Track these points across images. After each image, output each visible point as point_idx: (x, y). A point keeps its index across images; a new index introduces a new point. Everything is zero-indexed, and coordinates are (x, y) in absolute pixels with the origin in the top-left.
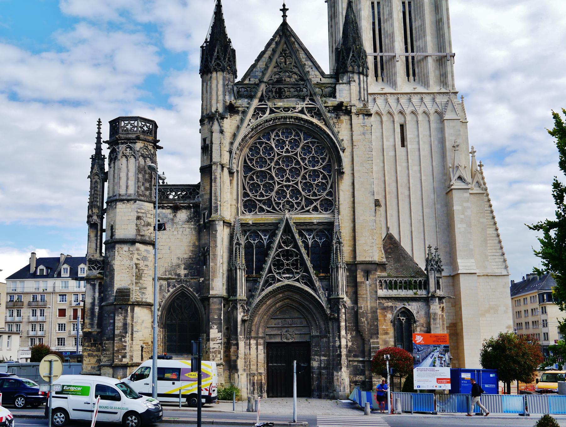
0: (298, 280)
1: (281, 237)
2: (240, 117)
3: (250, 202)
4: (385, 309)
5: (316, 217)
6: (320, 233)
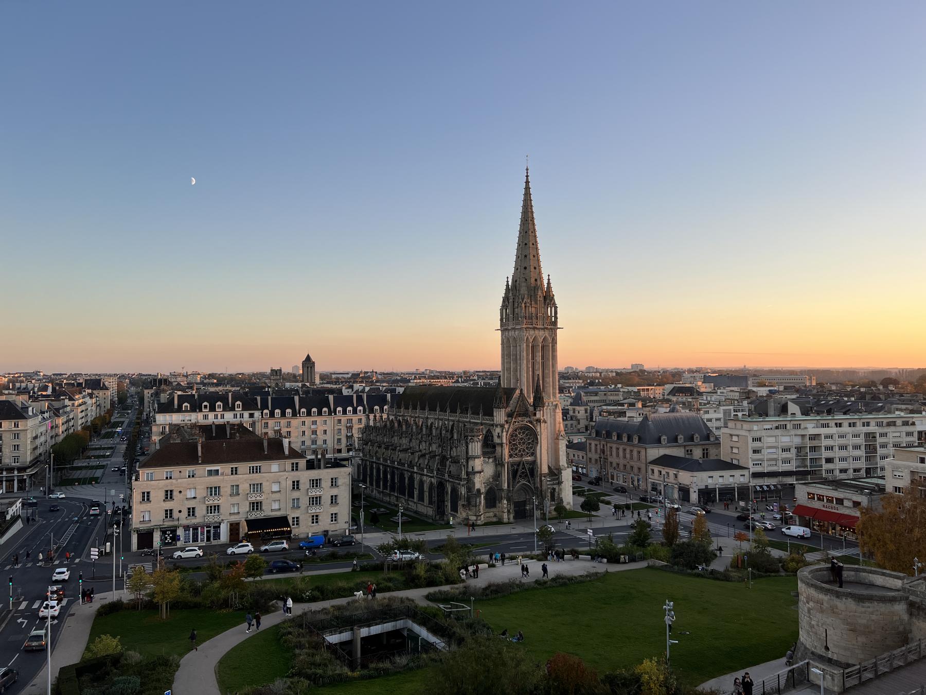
4: (548, 488)
6: (531, 464)
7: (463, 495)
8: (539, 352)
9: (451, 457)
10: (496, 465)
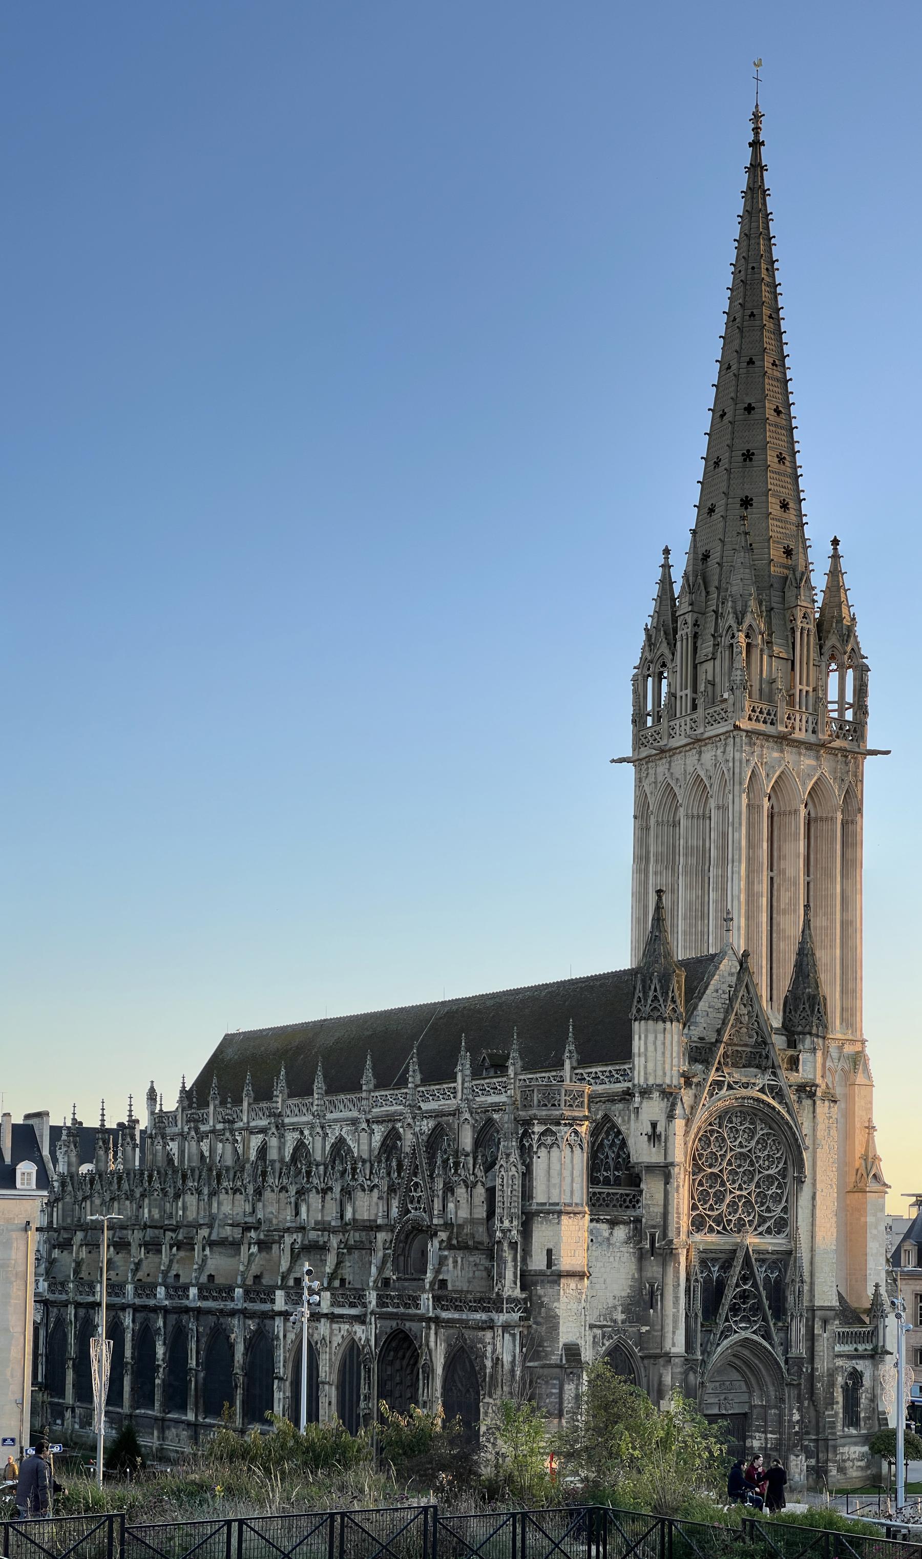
0: (754, 1332)
1: (740, 1273)
2: (694, 1091)
3: (697, 1218)
5: (772, 1243)
7: (507, 1366)
8: (797, 839)
9: (448, 1226)
10: (641, 1257)
